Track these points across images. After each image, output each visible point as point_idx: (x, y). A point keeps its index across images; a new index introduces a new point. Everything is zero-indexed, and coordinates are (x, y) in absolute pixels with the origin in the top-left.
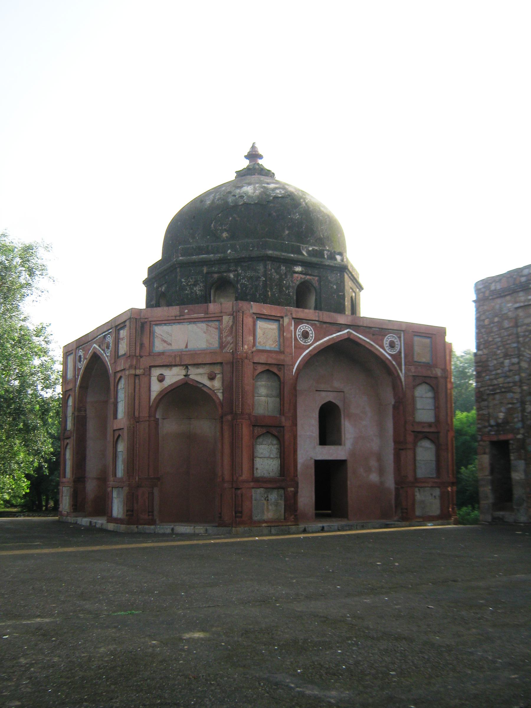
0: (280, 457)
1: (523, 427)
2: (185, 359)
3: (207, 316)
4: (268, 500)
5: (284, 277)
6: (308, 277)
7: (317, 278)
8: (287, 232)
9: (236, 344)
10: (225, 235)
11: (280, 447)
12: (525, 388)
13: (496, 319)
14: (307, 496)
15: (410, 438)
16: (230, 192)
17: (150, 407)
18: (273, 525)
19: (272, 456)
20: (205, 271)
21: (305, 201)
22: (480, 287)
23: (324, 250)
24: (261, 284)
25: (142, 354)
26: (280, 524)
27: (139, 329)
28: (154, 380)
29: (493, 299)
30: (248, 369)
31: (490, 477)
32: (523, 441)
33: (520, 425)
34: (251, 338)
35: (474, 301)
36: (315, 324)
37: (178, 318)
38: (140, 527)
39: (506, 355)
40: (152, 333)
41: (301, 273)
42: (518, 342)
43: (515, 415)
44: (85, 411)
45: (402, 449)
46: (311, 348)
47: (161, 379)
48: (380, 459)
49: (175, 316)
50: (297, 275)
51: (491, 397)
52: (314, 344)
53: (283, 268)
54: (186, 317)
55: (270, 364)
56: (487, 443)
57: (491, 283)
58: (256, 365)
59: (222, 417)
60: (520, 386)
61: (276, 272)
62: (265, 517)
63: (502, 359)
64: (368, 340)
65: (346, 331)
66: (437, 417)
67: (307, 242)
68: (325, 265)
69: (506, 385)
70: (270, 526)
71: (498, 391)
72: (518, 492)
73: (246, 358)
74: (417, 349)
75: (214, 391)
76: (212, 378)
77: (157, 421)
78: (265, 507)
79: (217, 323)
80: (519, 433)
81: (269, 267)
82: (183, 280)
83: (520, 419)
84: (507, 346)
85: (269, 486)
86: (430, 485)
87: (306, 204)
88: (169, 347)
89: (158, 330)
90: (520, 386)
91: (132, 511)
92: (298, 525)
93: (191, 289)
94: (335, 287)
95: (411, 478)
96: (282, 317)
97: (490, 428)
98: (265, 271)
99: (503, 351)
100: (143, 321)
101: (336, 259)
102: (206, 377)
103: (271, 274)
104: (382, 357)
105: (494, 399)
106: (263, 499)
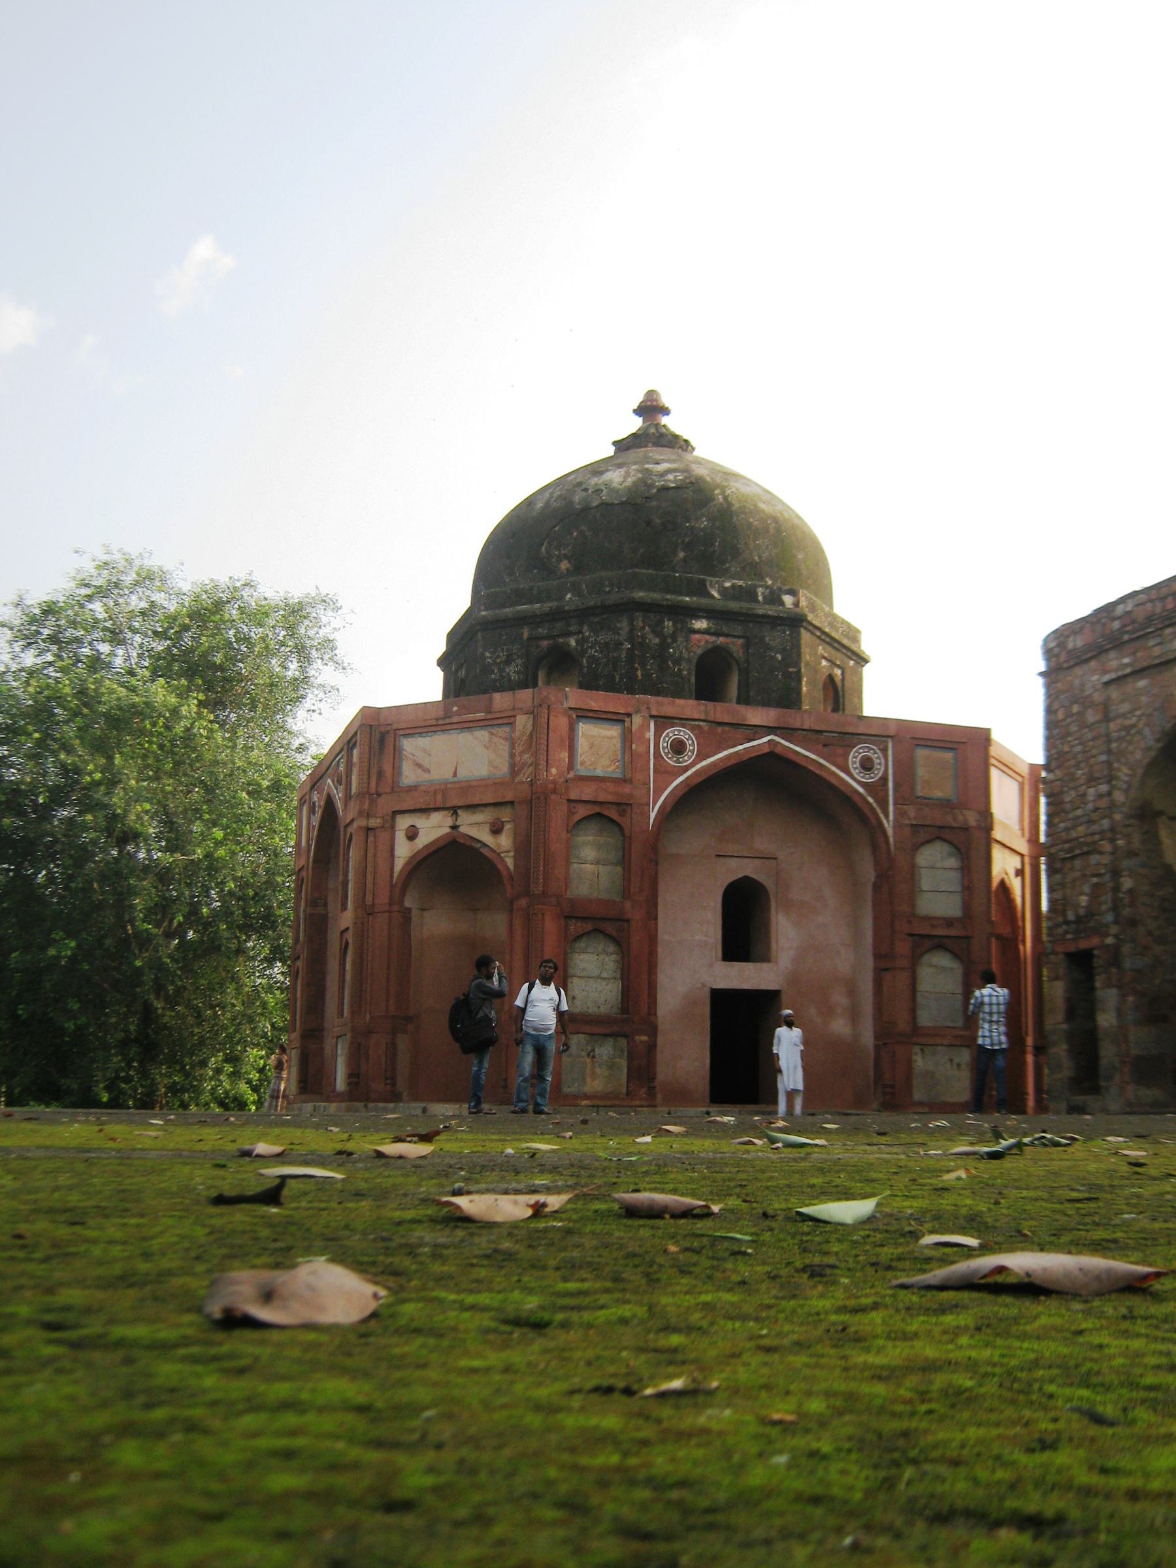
0: (622, 978)
1: (1116, 922)
2: (453, 799)
3: (490, 716)
4: (594, 1057)
5: (669, 640)
6: (721, 639)
7: (741, 641)
8: (682, 555)
9: (536, 764)
10: (564, 565)
11: (622, 958)
12: (1120, 842)
13: (1075, 709)
14: (687, 1054)
15: (903, 948)
16: (580, 484)
17: (392, 886)
18: (601, 1103)
19: (604, 975)
20: (526, 636)
21: (723, 493)
22: (1052, 645)
23: (756, 587)
24: (623, 655)
25: (381, 790)
26: (617, 1102)
27: (376, 745)
28: (400, 836)
29: (1069, 668)
30: (558, 814)
31: (1064, 1026)
32: (1116, 948)
33: (1110, 918)
34: (565, 755)
35: (1042, 674)
36: (699, 726)
37: (441, 722)
38: (371, 1105)
39: (1092, 780)
40: (397, 751)
41: (706, 632)
42: (1109, 752)
43: (1103, 899)
44: (326, 905)
45: (886, 970)
46: (689, 773)
47: (412, 834)
48: (852, 991)
49: (437, 719)
50: (697, 636)
51: (1068, 865)
52: (697, 764)
53: (668, 624)
54: (455, 719)
55: (601, 803)
56: (1061, 956)
57: (1068, 636)
58: (572, 805)
59: (511, 903)
60: (1112, 840)
61: (653, 632)
62: (587, 1089)
63: (1084, 787)
64: (813, 757)
65: (765, 739)
66: (966, 906)
67: (725, 573)
68: (758, 616)
69: (1089, 839)
70: (598, 1106)
71: (1077, 852)
72: (1108, 1053)
73: (554, 791)
74: (921, 772)
75: (499, 854)
76: (496, 830)
77: (406, 914)
78: (588, 1071)
79: (507, 729)
80: (1107, 935)
81: (639, 623)
82: (488, 654)
83: (1110, 905)
84: (1092, 761)
85: (597, 1030)
86: (946, 1042)
87: (726, 498)
88: (426, 776)
89: (409, 745)
90: (1112, 840)
91: (358, 1076)
92: (655, 1106)
93: (501, 670)
94: (779, 657)
95: (902, 1025)
96: (629, 715)
97: (1065, 927)
98: (632, 631)
99: (1086, 770)
100: (383, 729)
101: (782, 603)
102: (487, 828)
103: (643, 637)
104: (842, 788)
105: (1072, 869)
106: (584, 1054)
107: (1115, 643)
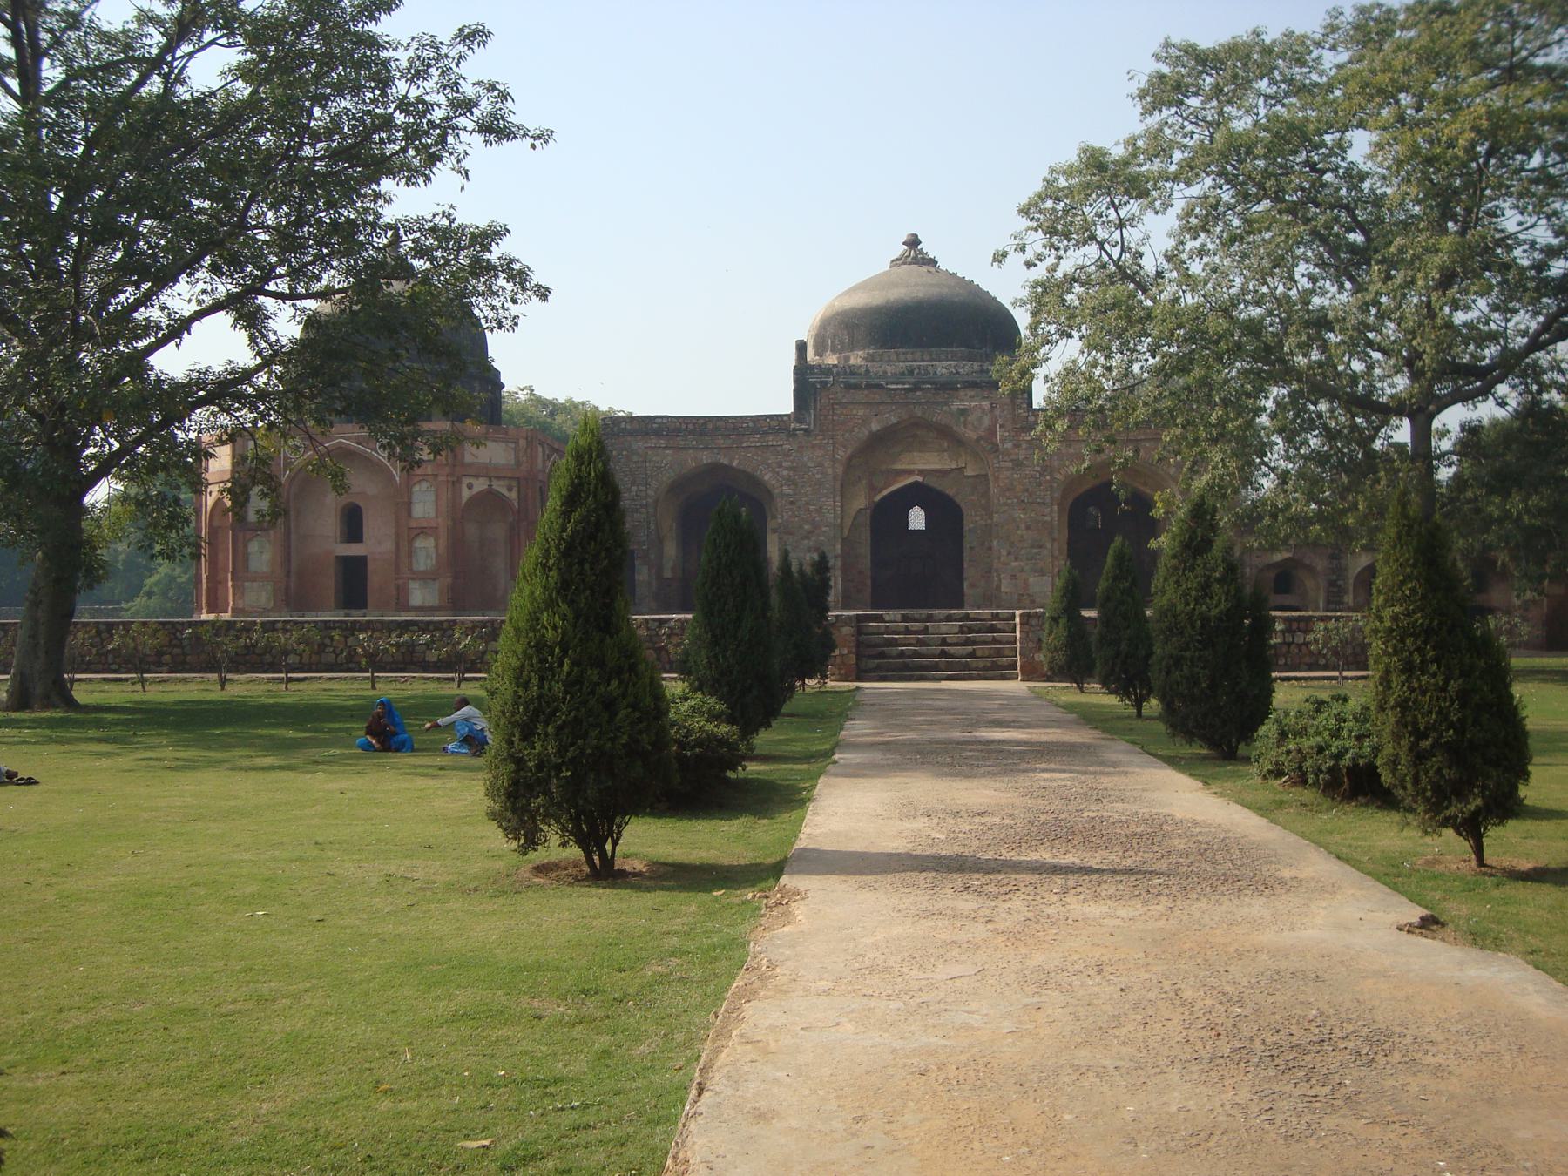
39: (633, 483)
47: (470, 486)
76: (510, 490)
107: (658, 433)
